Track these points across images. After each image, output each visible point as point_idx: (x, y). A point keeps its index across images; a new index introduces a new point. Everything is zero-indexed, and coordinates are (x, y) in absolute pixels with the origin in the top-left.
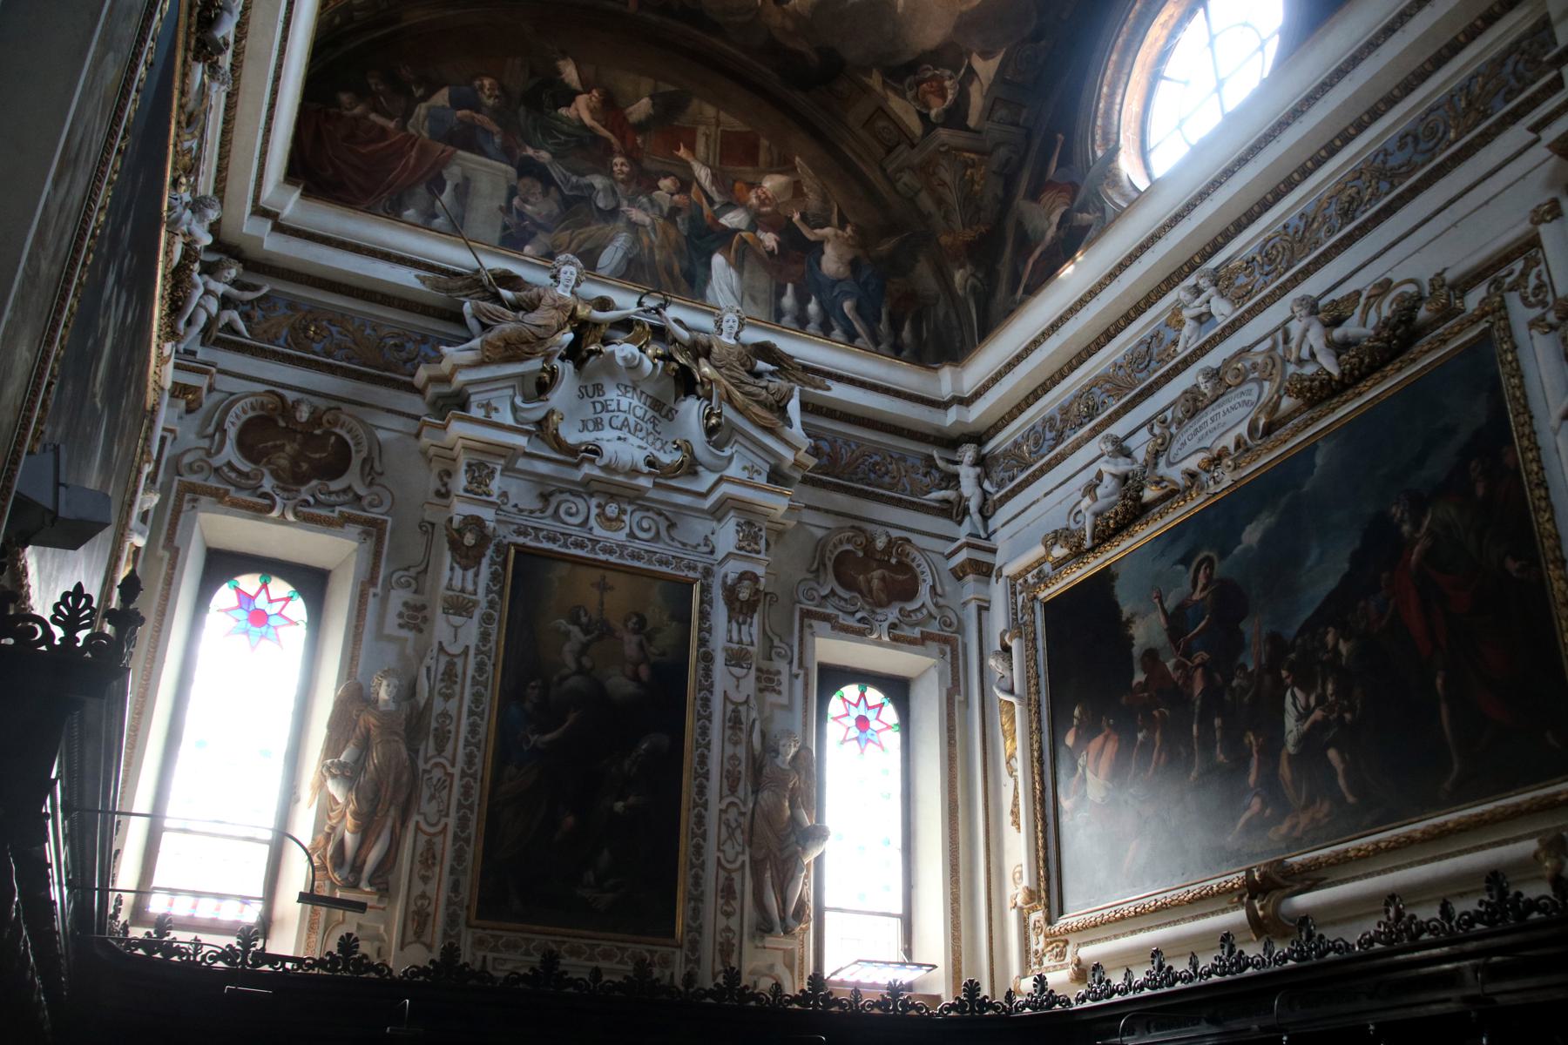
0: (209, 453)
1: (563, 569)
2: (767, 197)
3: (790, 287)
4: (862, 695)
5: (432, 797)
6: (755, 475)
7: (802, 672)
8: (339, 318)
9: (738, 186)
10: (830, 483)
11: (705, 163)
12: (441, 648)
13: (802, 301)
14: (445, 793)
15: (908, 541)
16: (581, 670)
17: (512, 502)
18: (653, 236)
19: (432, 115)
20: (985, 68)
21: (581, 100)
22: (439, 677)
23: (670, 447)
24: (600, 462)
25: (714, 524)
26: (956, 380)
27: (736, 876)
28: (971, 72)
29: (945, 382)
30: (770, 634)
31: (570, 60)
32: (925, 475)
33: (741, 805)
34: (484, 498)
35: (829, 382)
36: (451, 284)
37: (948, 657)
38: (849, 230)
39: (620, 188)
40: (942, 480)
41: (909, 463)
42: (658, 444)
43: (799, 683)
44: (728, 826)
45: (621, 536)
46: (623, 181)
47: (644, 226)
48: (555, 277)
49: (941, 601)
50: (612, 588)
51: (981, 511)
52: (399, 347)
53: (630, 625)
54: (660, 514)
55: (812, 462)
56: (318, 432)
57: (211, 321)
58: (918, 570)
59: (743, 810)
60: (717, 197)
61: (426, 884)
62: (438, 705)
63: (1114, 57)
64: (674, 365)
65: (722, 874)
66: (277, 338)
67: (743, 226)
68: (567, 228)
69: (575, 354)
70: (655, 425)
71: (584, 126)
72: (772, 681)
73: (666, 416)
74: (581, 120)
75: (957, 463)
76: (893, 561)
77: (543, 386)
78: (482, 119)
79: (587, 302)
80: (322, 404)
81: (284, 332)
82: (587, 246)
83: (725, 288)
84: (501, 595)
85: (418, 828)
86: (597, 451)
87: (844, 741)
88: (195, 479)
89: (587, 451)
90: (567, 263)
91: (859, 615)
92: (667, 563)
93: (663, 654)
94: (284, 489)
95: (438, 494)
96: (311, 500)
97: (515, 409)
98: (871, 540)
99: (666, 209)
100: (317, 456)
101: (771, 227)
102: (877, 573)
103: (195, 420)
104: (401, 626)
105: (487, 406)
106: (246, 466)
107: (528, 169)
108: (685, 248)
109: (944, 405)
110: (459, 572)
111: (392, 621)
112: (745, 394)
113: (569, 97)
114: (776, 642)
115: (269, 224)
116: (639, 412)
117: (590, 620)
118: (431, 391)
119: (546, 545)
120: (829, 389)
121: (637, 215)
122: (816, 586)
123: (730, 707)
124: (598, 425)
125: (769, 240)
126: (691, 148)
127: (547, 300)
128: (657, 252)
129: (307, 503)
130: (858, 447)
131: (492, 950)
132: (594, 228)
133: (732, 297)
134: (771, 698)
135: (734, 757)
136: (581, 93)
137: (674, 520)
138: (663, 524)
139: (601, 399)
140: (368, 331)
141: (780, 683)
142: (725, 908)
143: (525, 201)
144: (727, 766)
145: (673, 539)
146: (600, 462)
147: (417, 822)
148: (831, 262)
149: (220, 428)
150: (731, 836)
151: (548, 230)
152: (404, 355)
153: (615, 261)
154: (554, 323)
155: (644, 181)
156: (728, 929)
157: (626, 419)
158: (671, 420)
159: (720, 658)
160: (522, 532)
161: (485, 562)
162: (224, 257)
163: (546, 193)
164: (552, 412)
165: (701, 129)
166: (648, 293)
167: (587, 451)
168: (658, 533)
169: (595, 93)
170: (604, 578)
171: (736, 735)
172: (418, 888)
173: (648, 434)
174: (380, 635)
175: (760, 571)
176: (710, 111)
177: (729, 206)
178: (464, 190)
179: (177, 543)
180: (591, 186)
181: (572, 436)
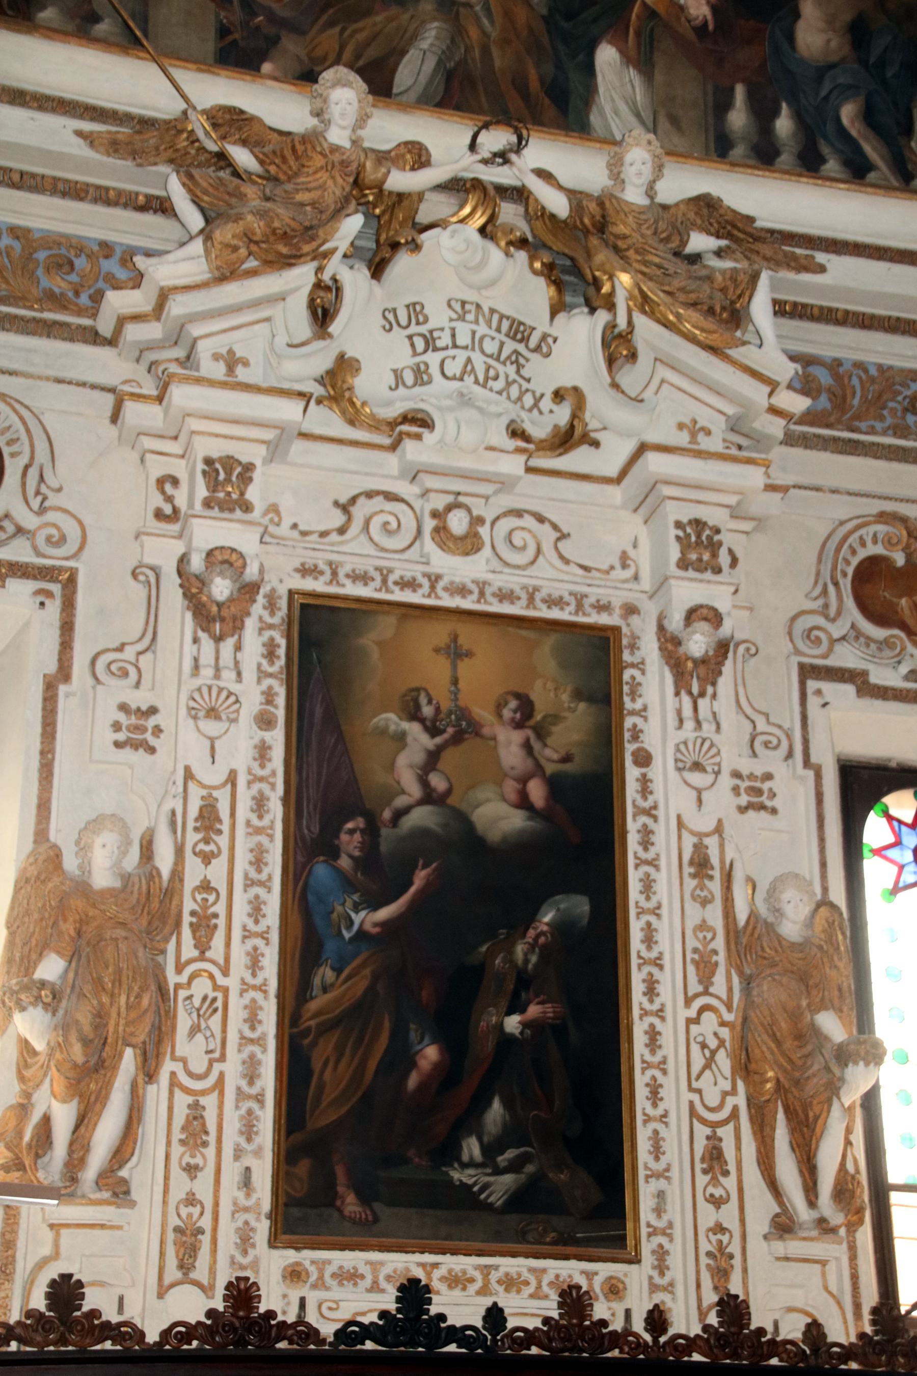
3: (740, 92)
5: (195, 1030)
6: (701, 437)
14: (215, 1022)
16: (429, 797)
17: (287, 523)
18: (486, 22)
22: (191, 824)
27: (726, 1133)
30: (749, 711)
33: (723, 1009)
35: (821, 257)
44: (704, 1046)
50: (469, 654)
53: (507, 713)
54: (541, 519)
55: (798, 404)
59: (729, 1017)
61: (193, 1178)
62: (194, 872)
65: (702, 1132)
68: (331, 24)
72: (759, 792)
73: (538, 349)
82: (372, 53)
83: (623, 108)
85: (174, 1082)
87: (896, 890)
90: (338, 83)
93: (567, 759)
108: (545, 40)
114: (762, 725)
116: (491, 347)
117: (438, 710)
120: (822, 269)
122: (820, 621)
123: (689, 842)
124: (421, 376)
128: (496, 52)
131: (314, 1287)
132: (379, 18)
133: (632, 119)
135: (703, 926)
137: (565, 531)
138: (547, 535)
139: (423, 329)
142: (710, 1190)
144: (691, 943)
145: (567, 562)
147: (173, 1074)
150: (709, 1063)
153: (423, 79)
156: (719, 1229)
157: (469, 360)
158: (548, 355)
161: (251, 624)
166: (486, 126)
170: (455, 638)
171: (702, 887)
172: (180, 1185)
173: (509, 384)
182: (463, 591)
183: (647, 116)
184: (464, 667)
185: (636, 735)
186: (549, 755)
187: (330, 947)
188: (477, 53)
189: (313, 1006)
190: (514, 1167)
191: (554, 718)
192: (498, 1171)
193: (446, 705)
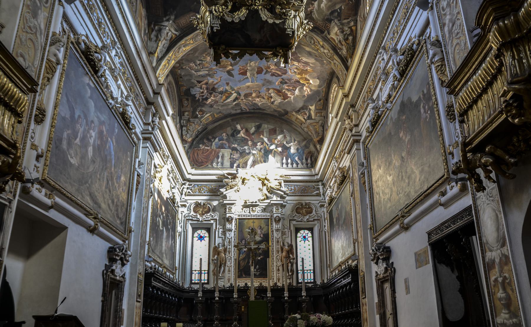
1: (247, 221)
3: (284, 158)
11: (266, 137)
13: (287, 160)
19: (215, 144)
20: (313, 108)
21: (241, 132)
26: (315, 170)
28: (310, 109)
35: (291, 177)
38: (296, 142)
39: (250, 148)
43: (290, 233)
45: (256, 213)
48: (237, 172)
49: (318, 213)
51: (323, 195)
60: (269, 144)
62: (228, 247)
65: (277, 267)
71: (243, 137)
80: (205, 201)
82: (245, 161)
92: (264, 216)
98: (302, 205)
101: (280, 147)
103: (186, 208)
106: (195, 214)
109: (314, 176)
113: (239, 132)
121: (254, 152)
125: (280, 149)
126: (263, 135)
134: (284, 236)
143: (233, 155)
148: (293, 150)
149: (190, 209)
151: (238, 160)
155: (255, 145)
159: (275, 231)
160: (239, 216)
163: (237, 153)
165: (265, 130)
174: (219, 237)
175: (279, 215)
176: (266, 126)
177: (271, 145)
178: (223, 157)
180: (245, 149)
182: (254, 216)
184: (255, 224)
186: (263, 232)
187: (242, 252)
191: (263, 228)
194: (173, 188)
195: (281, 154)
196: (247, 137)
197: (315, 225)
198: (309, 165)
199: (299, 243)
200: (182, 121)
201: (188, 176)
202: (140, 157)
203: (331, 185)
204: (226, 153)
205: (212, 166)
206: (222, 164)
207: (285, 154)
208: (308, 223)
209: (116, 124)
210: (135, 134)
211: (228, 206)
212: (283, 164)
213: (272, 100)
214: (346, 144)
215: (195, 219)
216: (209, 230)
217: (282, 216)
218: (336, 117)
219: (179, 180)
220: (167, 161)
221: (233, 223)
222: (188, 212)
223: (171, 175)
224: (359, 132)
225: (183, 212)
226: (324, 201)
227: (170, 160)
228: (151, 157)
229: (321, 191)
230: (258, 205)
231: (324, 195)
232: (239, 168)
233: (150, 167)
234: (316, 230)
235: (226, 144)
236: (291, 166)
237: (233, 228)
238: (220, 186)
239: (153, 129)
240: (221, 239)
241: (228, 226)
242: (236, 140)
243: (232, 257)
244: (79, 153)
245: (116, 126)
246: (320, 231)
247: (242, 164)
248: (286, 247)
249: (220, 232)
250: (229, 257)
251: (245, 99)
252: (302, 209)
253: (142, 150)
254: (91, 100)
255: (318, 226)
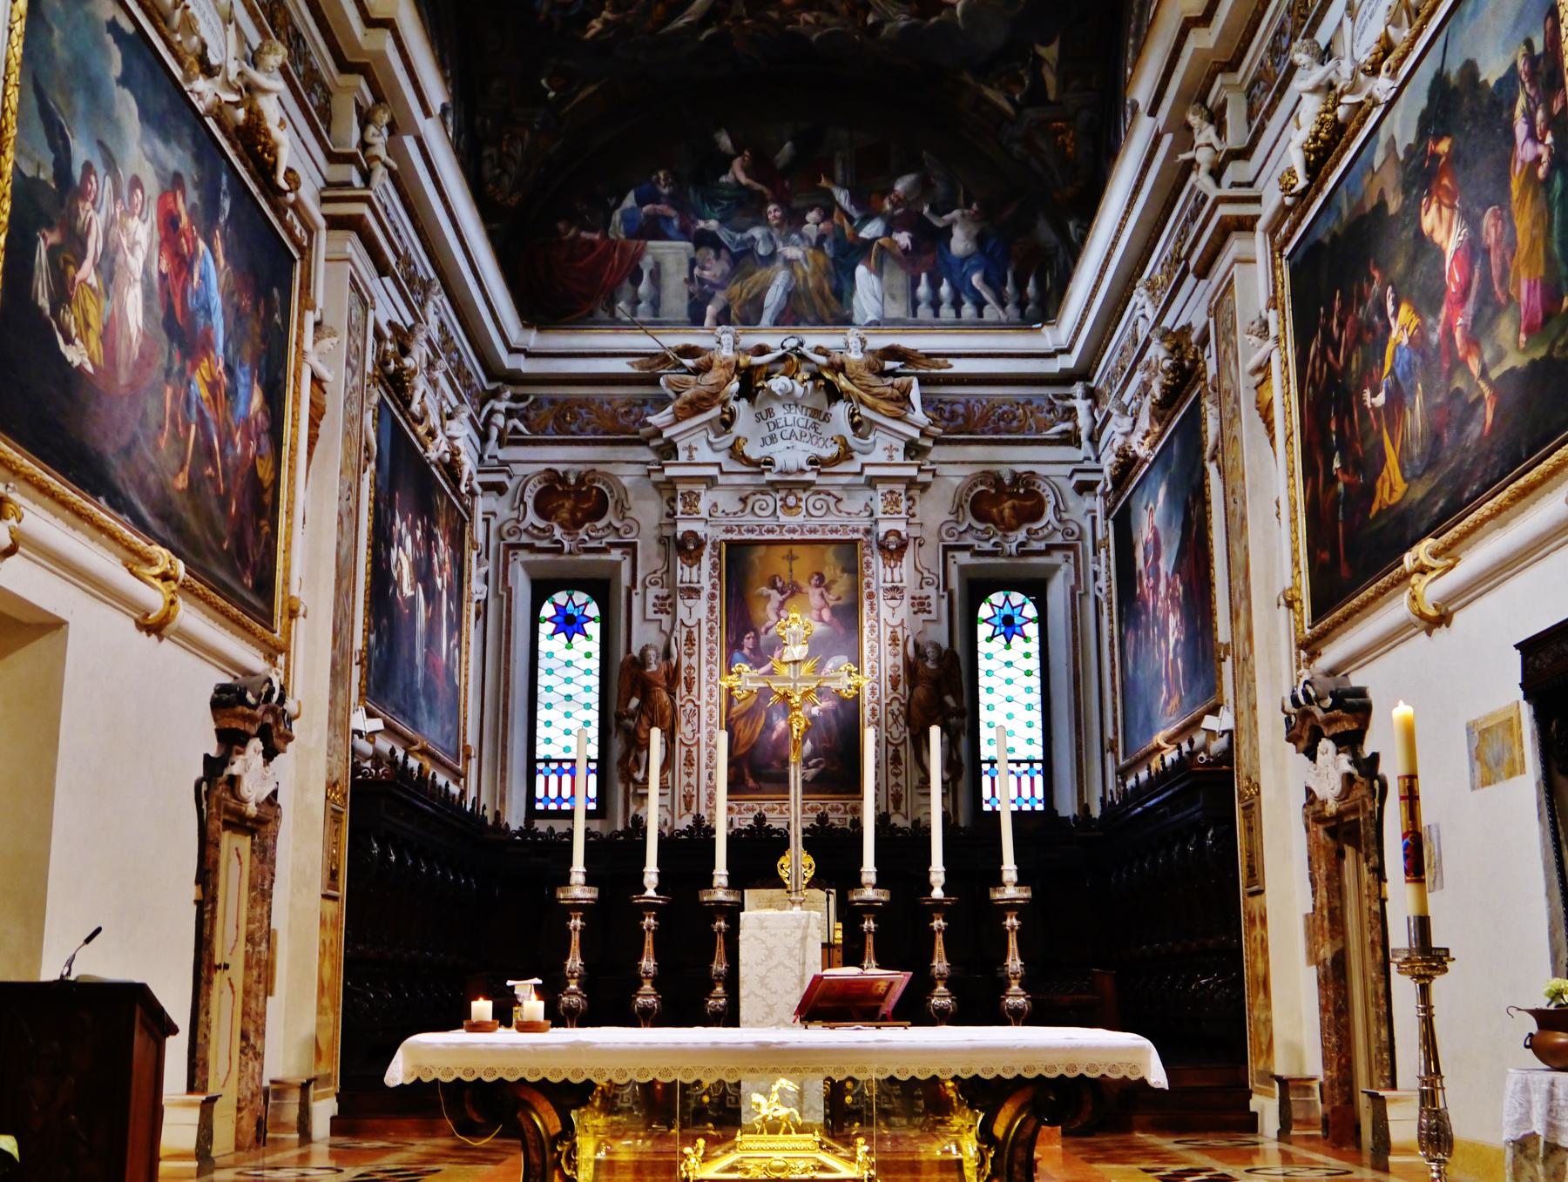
0: (518, 521)
1: (762, 550)
2: (899, 199)
3: (924, 277)
4: (1007, 598)
5: (688, 721)
6: (894, 453)
7: (946, 594)
8: (586, 402)
9: (873, 197)
10: (963, 440)
11: (843, 186)
12: (682, 623)
13: (935, 285)
15: (1033, 473)
17: (720, 509)
18: (805, 267)
19: (624, 219)
20: (1050, 53)
21: (737, 163)
23: (829, 443)
24: (778, 468)
25: (870, 493)
28: (1040, 61)
29: (1049, 338)
31: (724, 131)
32: (1049, 412)
34: (696, 516)
35: (950, 361)
36: (651, 363)
37: (1072, 560)
38: (975, 206)
40: (1064, 412)
41: (1035, 405)
42: (821, 442)
43: (944, 603)
44: (893, 714)
46: (777, 226)
47: (798, 260)
48: (719, 342)
49: (1065, 516)
50: (797, 558)
52: (627, 413)
53: (813, 582)
54: (829, 494)
56: (584, 489)
57: (501, 433)
58: (1044, 494)
60: (856, 215)
62: (685, 662)
63: (1131, 42)
64: (822, 383)
65: (891, 748)
66: (546, 427)
67: (880, 234)
69: (748, 391)
70: (816, 429)
72: (923, 604)
73: (824, 420)
74: (737, 181)
75: (1074, 398)
76: (1022, 491)
77: (727, 423)
78: (662, 208)
79: (746, 352)
81: (551, 422)
82: (755, 291)
83: (868, 295)
84: (720, 579)
86: (771, 463)
88: (512, 540)
89: (766, 463)
91: (992, 541)
92: (836, 531)
93: (838, 599)
94: (569, 534)
95: (668, 515)
96: (587, 538)
97: (710, 444)
98: (998, 480)
99: (814, 240)
100: (586, 506)
102: (1007, 505)
103: (506, 498)
104: (655, 612)
105: (690, 449)
106: (541, 524)
107: (704, 240)
108: (832, 268)
110: (686, 569)
111: (650, 609)
112: (874, 395)
115: (522, 357)
116: (802, 423)
118: (654, 443)
119: (747, 536)
120: (950, 366)
121: (792, 252)
122: (953, 525)
124: (773, 439)
125: (903, 239)
126: (832, 178)
127: (716, 362)
129: (584, 541)
130: (988, 402)
132: (758, 274)
136: (734, 157)
138: (832, 501)
140: (606, 407)
141: (929, 605)
143: (703, 268)
146: (775, 470)
148: (960, 243)
151: (721, 287)
152: (632, 418)
154: (723, 379)
155: (794, 220)
156: (897, 784)
162: (500, 384)
163: (718, 257)
164: (738, 438)
165: (838, 154)
167: (766, 463)
168: (828, 508)
169: (747, 153)
174: (645, 620)
175: (901, 527)
177: (866, 220)
178: (656, 275)
179: (510, 584)
180: (753, 239)
181: (754, 451)
182: (793, 531)
183: (880, 296)
184: (795, 564)
185: (868, 585)
188: (801, 282)
189: (734, 709)
190: (815, 766)
192: (809, 768)
193: (787, 581)
194: (450, 417)
195: (909, 260)
196: (758, 186)
197: (1056, 568)
198: (1030, 307)
199: (983, 647)
200: (478, 120)
201: (509, 362)
202: (320, 304)
203: (1126, 399)
204: (671, 255)
205: (613, 314)
206: (656, 304)
207: (926, 259)
208: (1022, 561)
209: (224, 178)
210: (297, 206)
211: (682, 488)
212: (915, 303)
213: (870, 20)
214: (1194, 230)
215: (545, 544)
216: (601, 589)
217: (915, 532)
218: (1153, 112)
219: (475, 380)
220: (422, 305)
221: (706, 562)
222: (515, 514)
223: (443, 364)
224: (1250, 185)
225: (494, 514)
226: (1095, 466)
227: (436, 299)
228: (362, 297)
229: (1083, 421)
230: (810, 484)
231: (1094, 438)
232: (729, 322)
233: (359, 342)
234: (1058, 592)
235: (669, 219)
236: (952, 313)
237: (706, 585)
238: (645, 402)
239: (366, 177)
240: (655, 626)
241: (684, 573)
242: (713, 202)
243: (702, 703)
244: (92, 321)
245: (224, 187)
246: (1075, 597)
247: (741, 307)
248: (929, 664)
249: (651, 599)
250: (690, 706)
251: (749, 17)
252: (997, 500)
253: (326, 271)
254: (126, 93)
255: (1066, 575)
